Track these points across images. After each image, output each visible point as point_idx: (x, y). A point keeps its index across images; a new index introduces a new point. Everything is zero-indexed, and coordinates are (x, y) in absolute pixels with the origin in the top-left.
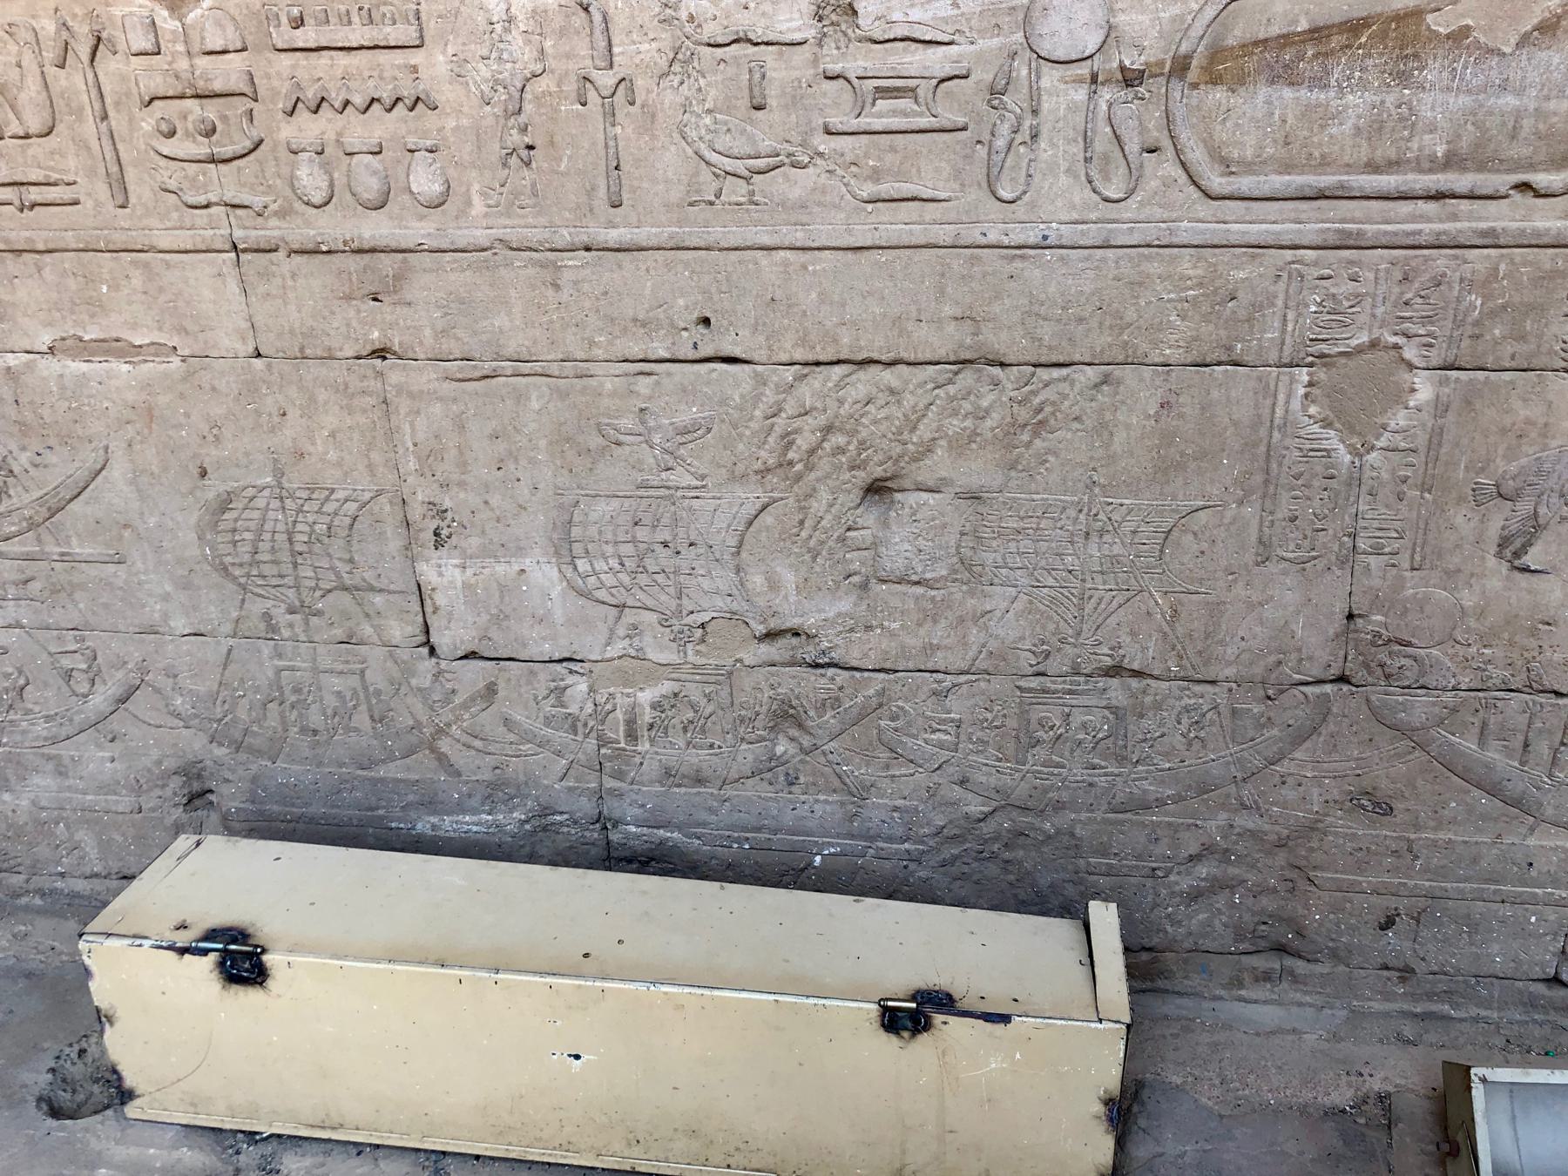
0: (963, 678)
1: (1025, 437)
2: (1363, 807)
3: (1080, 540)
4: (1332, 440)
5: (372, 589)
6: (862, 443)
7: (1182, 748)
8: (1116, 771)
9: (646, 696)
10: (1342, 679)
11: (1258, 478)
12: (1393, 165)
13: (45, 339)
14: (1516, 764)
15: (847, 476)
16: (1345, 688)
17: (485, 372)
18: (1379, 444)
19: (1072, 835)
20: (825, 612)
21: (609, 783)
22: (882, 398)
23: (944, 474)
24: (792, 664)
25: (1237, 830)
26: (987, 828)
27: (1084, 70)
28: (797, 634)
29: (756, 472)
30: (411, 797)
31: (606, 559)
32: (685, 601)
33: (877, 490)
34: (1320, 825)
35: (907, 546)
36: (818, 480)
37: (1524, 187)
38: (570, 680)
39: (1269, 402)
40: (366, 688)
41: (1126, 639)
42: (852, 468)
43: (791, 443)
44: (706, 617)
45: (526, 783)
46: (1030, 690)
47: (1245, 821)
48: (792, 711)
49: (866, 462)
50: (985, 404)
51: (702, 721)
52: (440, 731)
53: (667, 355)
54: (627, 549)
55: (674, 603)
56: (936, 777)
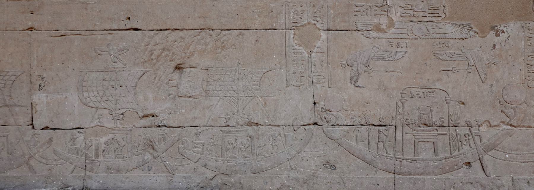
0: (204, 128)
1: (220, 51)
2: (327, 167)
3: (236, 81)
4: (302, 50)
5: (16, 105)
6: (173, 53)
7: (271, 149)
8: (252, 158)
9: (103, 140)
10: (315, 124)
11: (284, 61)
14: (367, 149)
15: (169, 63)
16: (316, 126)
17: (62, 34)
18: (314, 51)
19: (240, 183)
20: (162, 109)
21: (88, 173)
22: (179, 40)
23: (197, 62)
24: (151, 126)
25: (291, 178)
26: (214, 183)
28: (153, 116)
29: (142, 62)
30: (17, 183)
31: (93, 92)
32: (118, 105)
33: (178, 68)
34: (315, 174)
35: (187, 85)
36: (160, 65)
38: (78, 135)
39: (284, 40)
40: (7, 141)
41: (252, 112)
42: (171, 61)
43: (153, 53)
44: (124, 111)
45: (59, 175)
46: (225, 131)
47: (293, 175)
48: (151, 143)
49: (174, 59)
50: (208, 41)
51: (121, 148)
52: (32, 157)
53: (117, 28)
54: (100, 88)
55: (114, 106)
56: (197, 164)
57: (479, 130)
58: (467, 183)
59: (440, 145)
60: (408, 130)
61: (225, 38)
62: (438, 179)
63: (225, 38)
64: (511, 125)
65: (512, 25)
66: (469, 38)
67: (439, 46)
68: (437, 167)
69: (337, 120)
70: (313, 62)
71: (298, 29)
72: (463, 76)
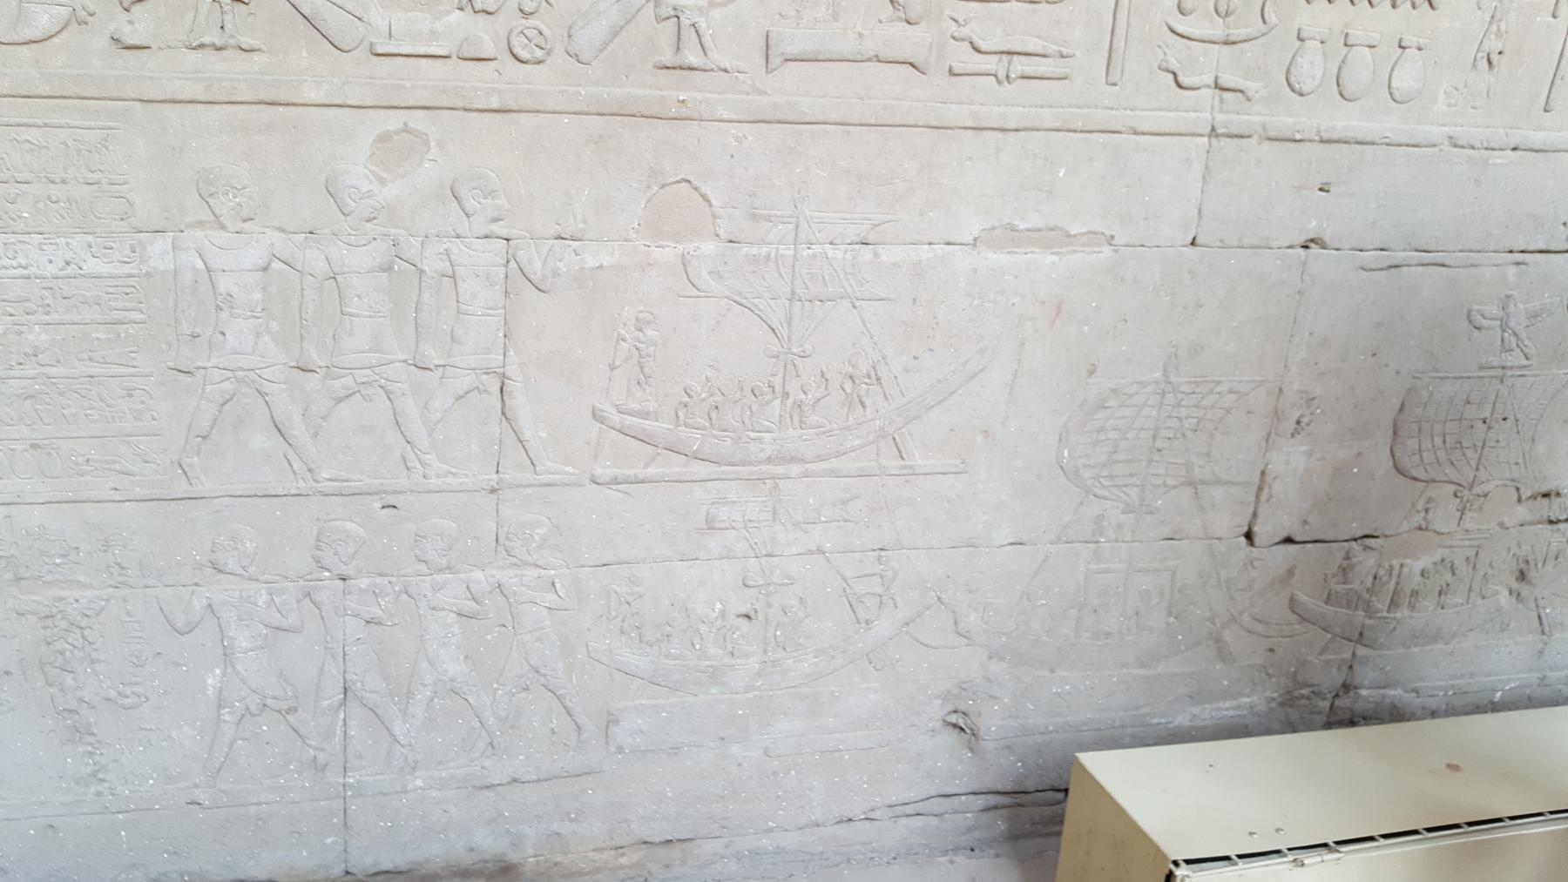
13: (974, 230)
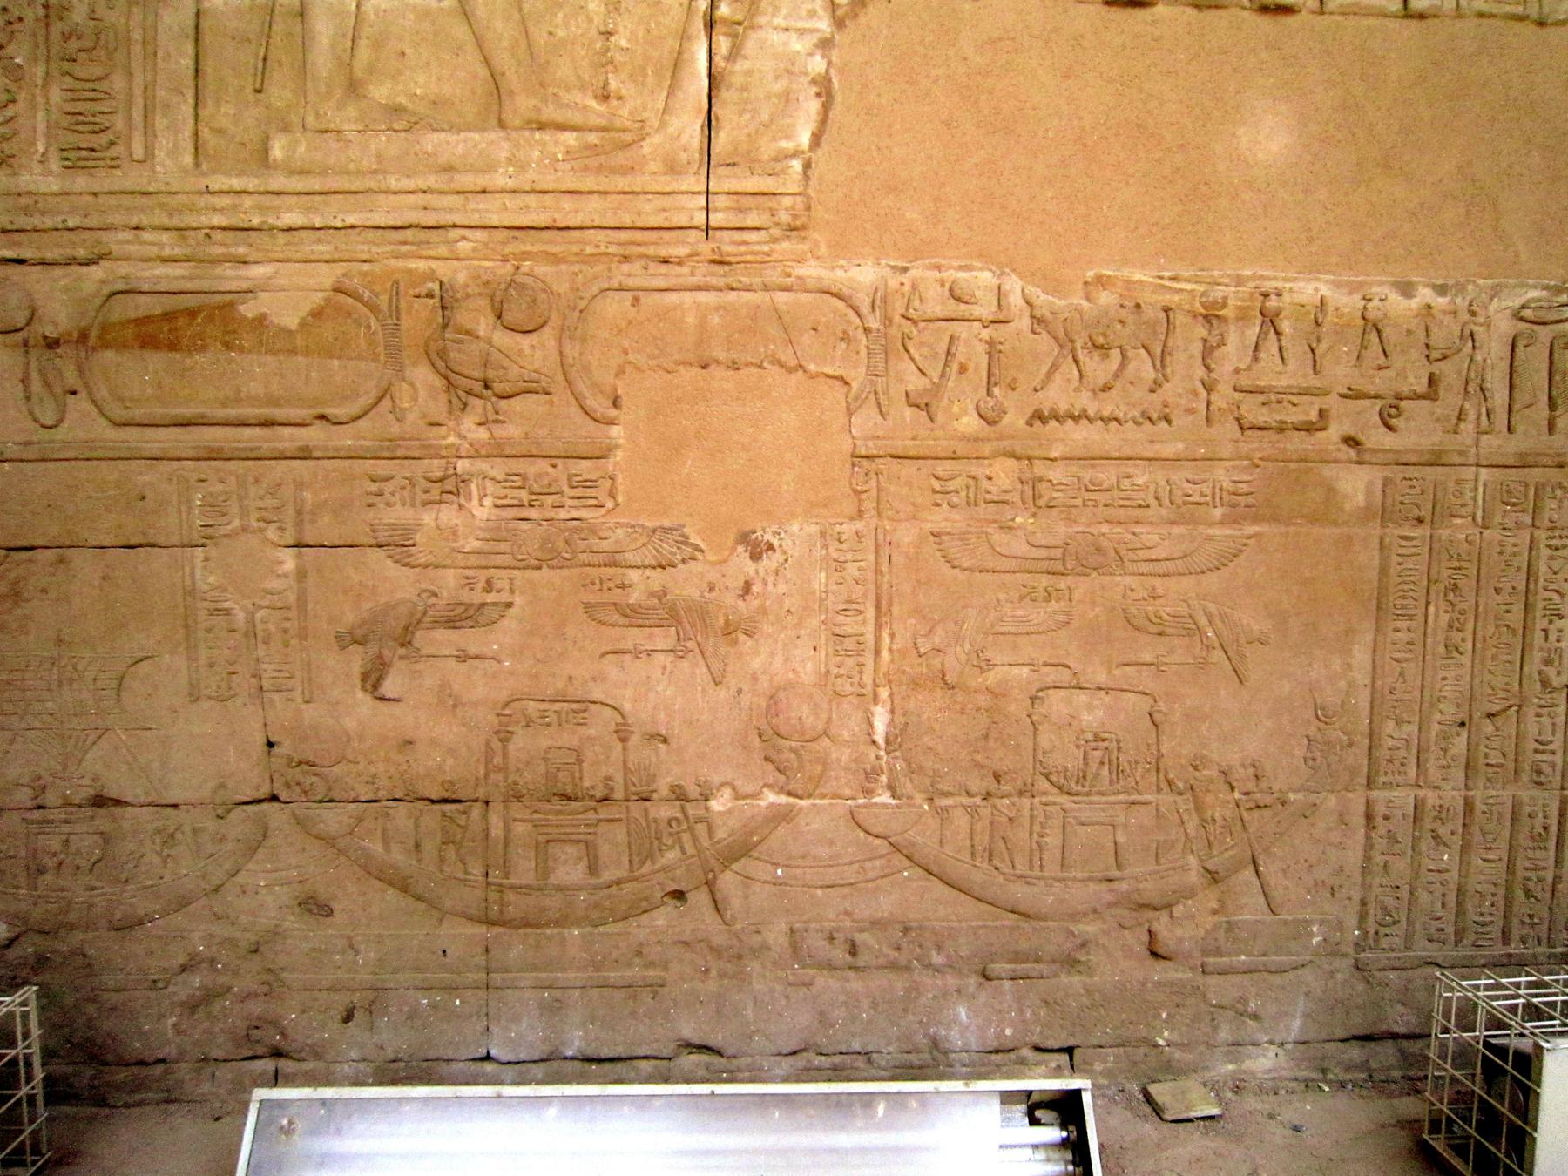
10: (274, 798)
12: (237, 401)
16: (276, 805)
27: (19, 337)
37: (322, 417)
46: (32, 822)
47: (218, 929)
57: (707, 808)
58: (675, 943)
59: (604, 849)
60: (517, 810)
61: (20, 571)
62: (600, 934)
63: (20, 571)
64: (790, 794)
65: (795, 528)
66: (680, 566)
67: (597, 587)
68: (596, 905)
69: (330, 789)
70: (260, 635)
71: (216, 545)
72: (665, 668)
